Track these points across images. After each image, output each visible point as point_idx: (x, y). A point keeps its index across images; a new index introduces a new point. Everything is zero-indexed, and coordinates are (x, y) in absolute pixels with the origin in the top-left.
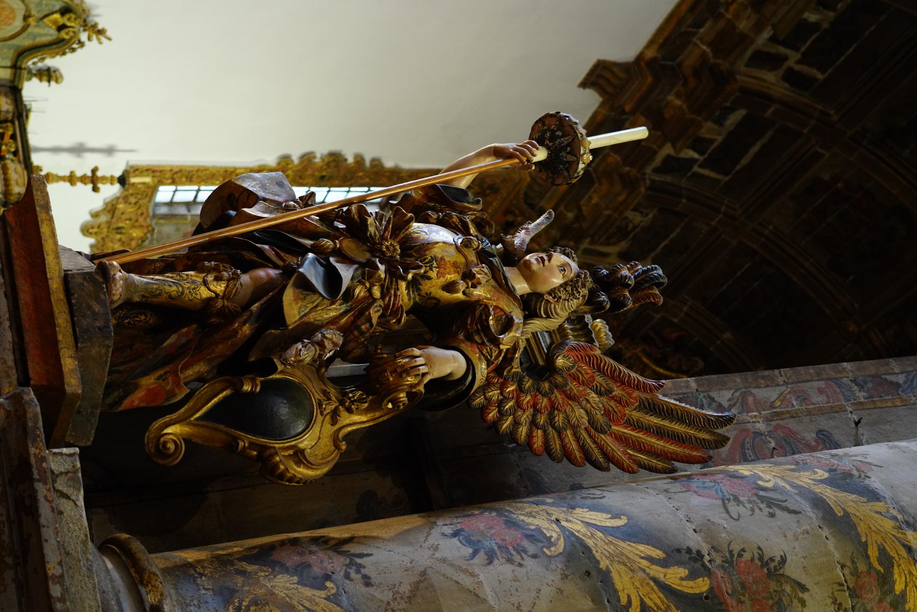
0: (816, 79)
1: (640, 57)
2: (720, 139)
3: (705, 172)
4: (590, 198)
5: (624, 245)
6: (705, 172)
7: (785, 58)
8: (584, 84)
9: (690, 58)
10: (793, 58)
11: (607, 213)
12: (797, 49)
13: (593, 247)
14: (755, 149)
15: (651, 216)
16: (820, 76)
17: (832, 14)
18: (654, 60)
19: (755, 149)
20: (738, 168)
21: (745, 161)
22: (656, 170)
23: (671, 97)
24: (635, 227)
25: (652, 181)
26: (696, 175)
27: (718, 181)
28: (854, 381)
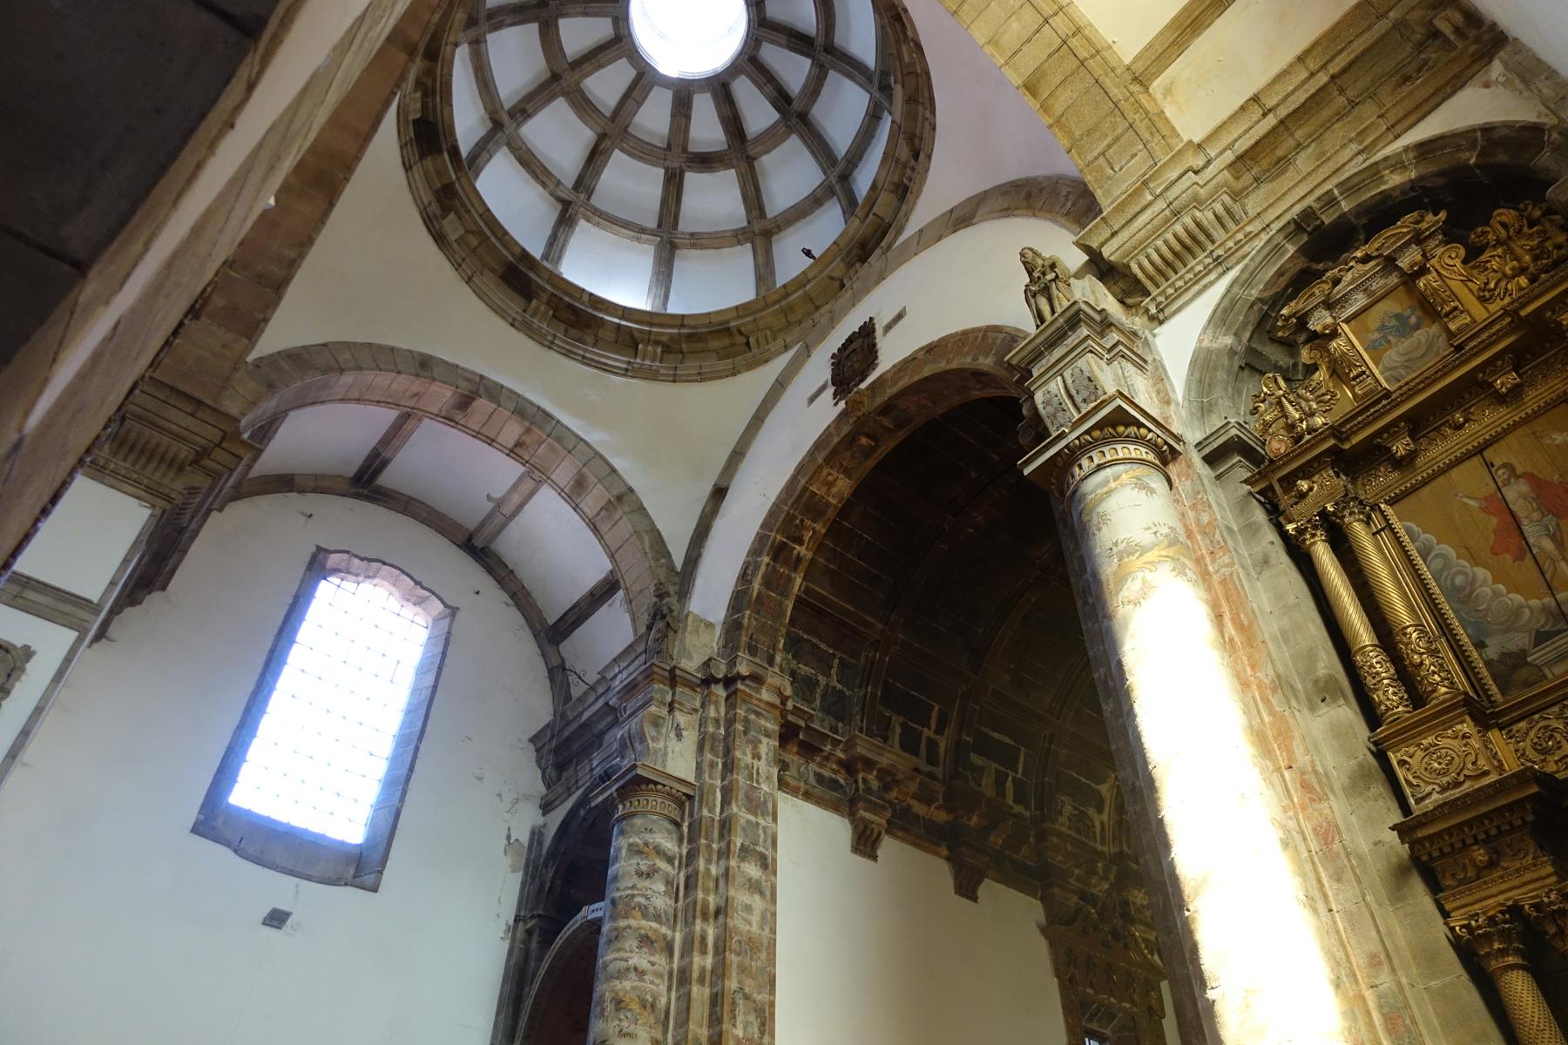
0: (940, 710)
1: (948, 859)
2: (994, 765)
3: (1020, 770)
4: (1060, 862)
5: (1091, 812)
6: (1020, 770)
7: (929, 739)
8: (975, 899)
9: (942, 817)
10: (928, 733)
11: (1069, 848)
12: (921, 732)
13: (1098, 839)
14: (996, 735)
15: (1063, 798)
16: (937, 707)
17: (894, 718)
18: (949, 848)
19: (996, 735)
20: (1013, 743)
21: (1007, 740)
22: (1027, 807)
23: (972, 824)
24: (1076, 808)
25: (1035, 810)
26: (1024, 774)
27: (1026, 755)
28: (1169, 935)
